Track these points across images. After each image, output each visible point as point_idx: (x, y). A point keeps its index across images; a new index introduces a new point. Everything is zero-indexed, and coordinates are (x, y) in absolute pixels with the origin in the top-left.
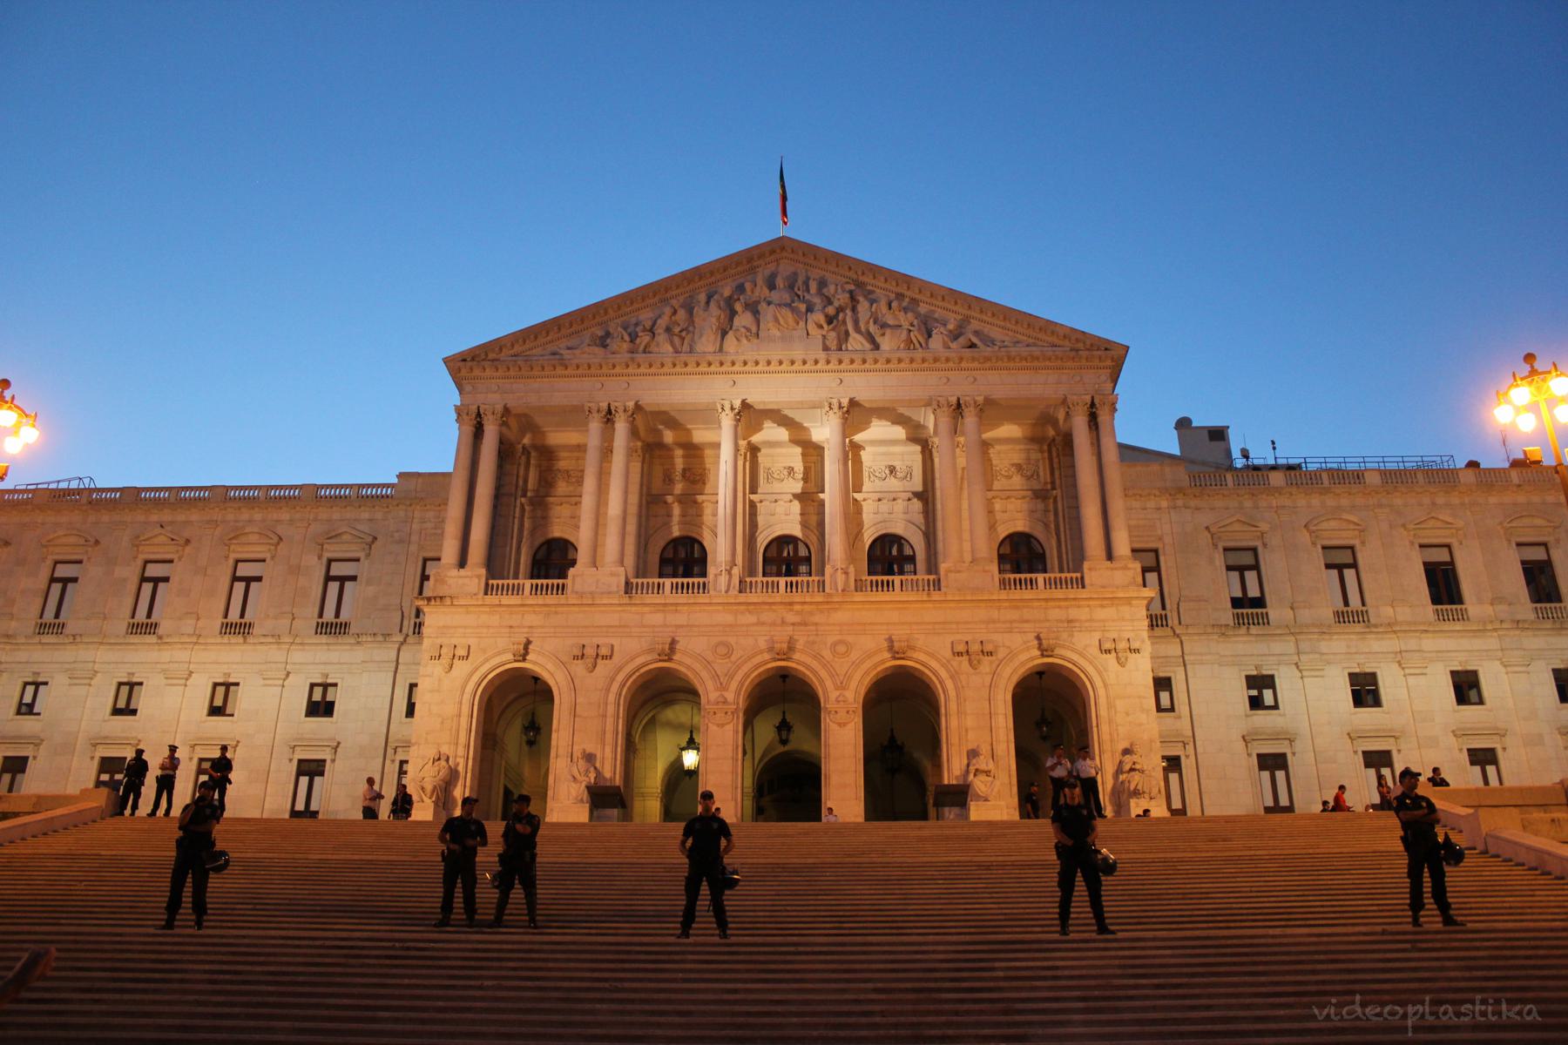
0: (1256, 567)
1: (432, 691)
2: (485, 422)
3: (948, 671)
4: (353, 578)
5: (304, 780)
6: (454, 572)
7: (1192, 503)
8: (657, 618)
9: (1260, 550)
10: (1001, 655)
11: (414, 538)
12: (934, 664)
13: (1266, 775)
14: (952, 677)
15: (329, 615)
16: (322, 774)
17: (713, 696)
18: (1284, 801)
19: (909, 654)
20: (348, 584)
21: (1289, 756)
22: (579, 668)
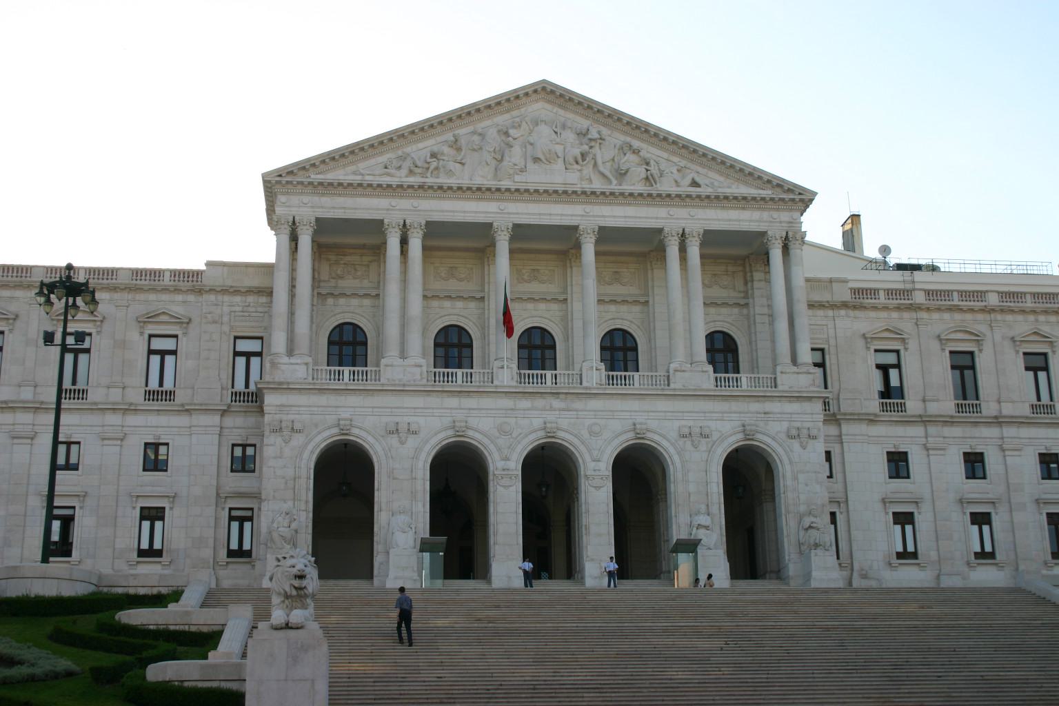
0: (898, 366)
1: (275, 458)
2: (299, 231)
3: (675, 448)
4: (174, 353)
5: (146, 524)
6: (285, 359)
7: (851, 313)
8: (453, 402)
9: (902, 353)
10: (715, 438)
11: (226, 319)
12: (665, 443)
13: (898, 527)
14: (679, 453)
15: (154, 384)
16: (162, 519)
17: (500, 464)
18: (910, 548)
19: (649, 435)
20: (169, 359)
21: (916, 515)
22: (394, 440)
